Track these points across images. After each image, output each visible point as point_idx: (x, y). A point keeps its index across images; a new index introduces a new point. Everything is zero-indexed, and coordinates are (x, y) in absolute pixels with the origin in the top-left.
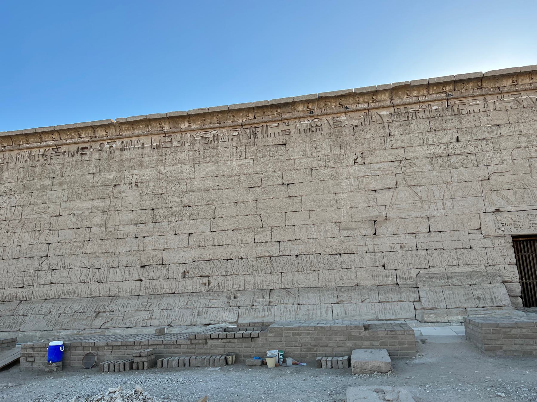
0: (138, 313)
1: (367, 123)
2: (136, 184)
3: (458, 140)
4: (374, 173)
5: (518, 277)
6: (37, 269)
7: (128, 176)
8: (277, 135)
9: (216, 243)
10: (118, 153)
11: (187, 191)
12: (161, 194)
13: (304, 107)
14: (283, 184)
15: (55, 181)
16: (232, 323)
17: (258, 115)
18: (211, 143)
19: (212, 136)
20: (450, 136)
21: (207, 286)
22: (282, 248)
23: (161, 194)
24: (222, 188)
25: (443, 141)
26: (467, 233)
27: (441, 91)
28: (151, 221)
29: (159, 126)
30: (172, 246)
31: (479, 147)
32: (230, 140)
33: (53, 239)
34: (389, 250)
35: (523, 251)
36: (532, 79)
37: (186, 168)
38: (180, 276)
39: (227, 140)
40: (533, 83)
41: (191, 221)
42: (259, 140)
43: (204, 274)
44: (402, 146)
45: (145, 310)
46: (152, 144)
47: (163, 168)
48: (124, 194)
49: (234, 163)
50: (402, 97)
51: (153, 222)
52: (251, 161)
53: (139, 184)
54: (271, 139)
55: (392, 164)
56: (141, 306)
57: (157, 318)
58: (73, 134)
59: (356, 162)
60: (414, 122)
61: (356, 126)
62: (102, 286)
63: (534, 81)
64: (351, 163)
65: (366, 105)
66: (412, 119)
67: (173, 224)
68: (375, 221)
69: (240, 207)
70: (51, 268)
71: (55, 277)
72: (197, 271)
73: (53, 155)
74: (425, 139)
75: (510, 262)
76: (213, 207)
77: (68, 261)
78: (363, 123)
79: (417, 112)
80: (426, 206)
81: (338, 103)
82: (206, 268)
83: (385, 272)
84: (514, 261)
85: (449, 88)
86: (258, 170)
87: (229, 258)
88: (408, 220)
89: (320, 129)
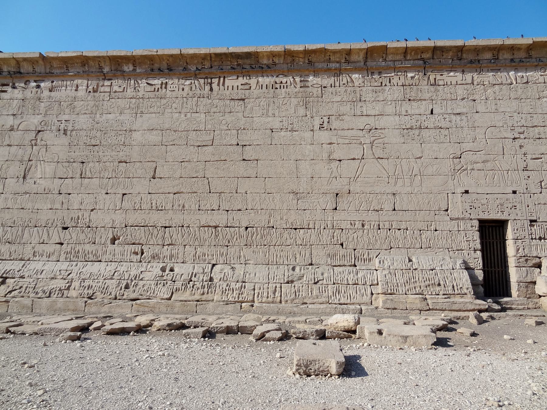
0: (53, 281)
1: (337, 84)
2: (65, 133)
3: (432, 113)
4: (340, 141)
5: (481, 264)
8: (235, 88)
9: (154, 208)
10: (46, 93)
11: (124, 145)
13: (269, 60)
14: (238, 145)
16: (164, 299)
17: (216, 63)
19: (160, 82)
20: (424, 107)
21: (139, 256)
22: (230, 218)
24: (166, 144)
25: (417, 112)
26: (432, 213)
27: (419, 57)
28: (78, 175)
29: (97, 66)
30: (101, 207)
31: (454, 122)
32: (181, 90)
34: (349, 226)
35: (487, 238)
36: (513, 54)
37: (126, 117)
38: (109, 242)
39: (177, 89)
41: (127, 179)
42: (215, 92)
43: (137, 242)
44: (373, 112)
45: (62, 278)
46: (88, 87)
47: (98, 116)
48: (48, 143)
49: (183, 116)
50: (377, 60)
52: (203, 116)
53: (69, 133)
54: (228, 93)
55: (360, 133)
56: (58, 273)
57: (76, 288)
59: (321, 127)
60: (387, 88)
61: (325, 87)
62: (13, 248)
63: (515, 56)
64: (317, 127)
65: (338, 65)
66: (386, 85)
67: (105, 181)
68: (337, 194)
69: (185, 168)
72: (129, 237)
74: (398, 108)
75: (474, 248)
76: (154, 166)
78: (333, 85)
79: (391, 78)
80: (392, 181)
81: (307, 59)
82: (140, 235)
83: (342, 252)
84: (479, 246)
85: (428, 56)
86: (210, 126)
87: (167, 225)
88: (372, 195)
89: (285, 87)
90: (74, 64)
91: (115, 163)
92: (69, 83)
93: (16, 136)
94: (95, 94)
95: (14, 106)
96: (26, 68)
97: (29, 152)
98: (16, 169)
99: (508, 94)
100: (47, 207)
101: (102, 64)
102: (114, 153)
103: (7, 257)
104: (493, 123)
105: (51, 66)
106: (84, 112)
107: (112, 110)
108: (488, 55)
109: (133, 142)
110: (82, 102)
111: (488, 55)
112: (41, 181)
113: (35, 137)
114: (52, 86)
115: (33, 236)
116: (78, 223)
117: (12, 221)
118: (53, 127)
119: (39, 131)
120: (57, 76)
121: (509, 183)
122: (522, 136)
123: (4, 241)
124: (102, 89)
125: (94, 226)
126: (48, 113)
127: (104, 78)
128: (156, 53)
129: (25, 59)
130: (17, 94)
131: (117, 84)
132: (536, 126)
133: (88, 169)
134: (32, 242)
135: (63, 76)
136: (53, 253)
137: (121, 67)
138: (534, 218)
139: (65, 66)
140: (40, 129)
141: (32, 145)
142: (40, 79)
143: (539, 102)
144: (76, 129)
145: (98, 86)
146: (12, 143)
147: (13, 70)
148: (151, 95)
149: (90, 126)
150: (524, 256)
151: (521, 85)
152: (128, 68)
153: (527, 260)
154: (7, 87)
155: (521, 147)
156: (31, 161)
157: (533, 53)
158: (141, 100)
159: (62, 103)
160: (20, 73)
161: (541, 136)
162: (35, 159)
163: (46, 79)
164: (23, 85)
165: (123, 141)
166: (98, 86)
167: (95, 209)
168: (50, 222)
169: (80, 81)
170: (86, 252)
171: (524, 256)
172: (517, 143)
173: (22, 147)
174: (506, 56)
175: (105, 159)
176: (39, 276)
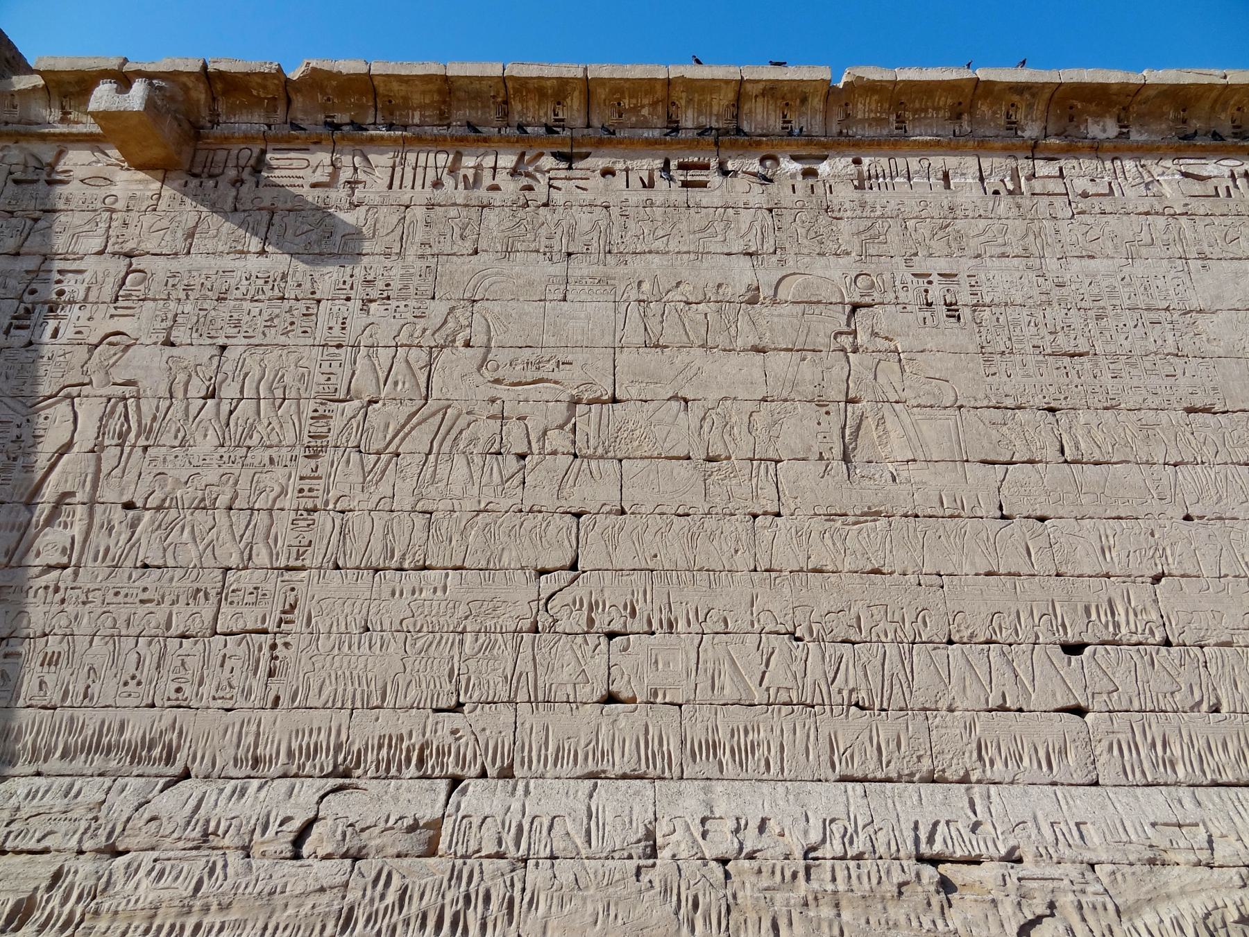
2: (952, 310)
6: (526, 624)
7: (909, 278)
10: (845, 194)
12: (1072, 356)
15: (580, 268)
18: (1229, 195)
23: (1072, 356)
28: (1052, 453)
29: (1002, 122)
33: (594, 491)
51: (1066, 461)
53: (966, 313)
58: (645, 112)
62: (885, 729)
70: (601, 623)
71: (633, 666)
73: (562, 174)
77: (688, 599)
90: (926, 110)
91: (1172, 414)
92: (914, 164)
93: (777, 322)
94: (1018, 199)
95: (744, 227)
96: (761, 117)
97: (839, 371)
98: (801, 429)
100: (973, 564)
101: (1020, 116)
102: (1154, 381)
103: (871, 768)
105: (848, 116)
106: (999, 250)
107: (1094, 247)
109: (1208, 347)
110: (982, 223)
112: (915, 473)
113: (848, 325)
114: (860, 173)
115: (965, 678)
116: (1117, 626)
117: (849, 617)
118: (902, 295)
119: (855, 307)
120: (875, 145)
123: (836, 698)
124: (1037, 185)
125: (1188, 638)
126: (871, 251)
127: (1030, 155)
128: (1223, 81)
129: (772, 90)
130: (744, 190)
131: (1082, 173)
133: (1080, 433)
134: (958, 703)
135: (895, 144)
136: (1063, 752)
137: (1078, 127)
139: (893, 118)
140: (857, 299)
141: (843, 350)
142: (815, 151)
144: (987, 300)
145: (1015, 177)
146: (766, 341)
147: (714, 125)
148: (1201, 207)
149: (1035, 292)
152: (1104, 131)
154: (706, 172)
156: (854, 401)
158: (1183, 221)
159: (911, 223)
160: (739, 131)
162: (871, 397)
163: (831, 153)
164: (755, 166)
165: (1170, 341)
166: (1015, 177)
167: (1163, 575)
168: (1008, 621)
169: (951, 162)
170: (1200, 744)
173: (809, 355)
175: (1131, 400)
176: (1088, 856)
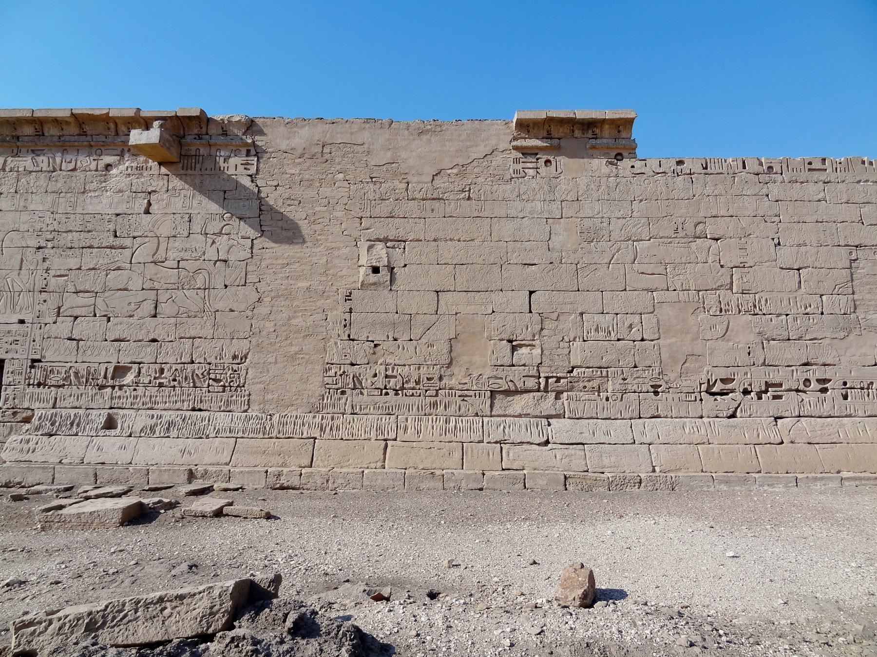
40: (63, 136)
63: (65, 132)
99: (45, 185)
104: (17, 226)
108: (28, 130)
111: (28, 130)
121: (18, 308)
122: (50, 245)
132: (71, 231)
138: (38, 357)
143: (81, 198)
150: (13, 408)
151: (65, 173)
153: (15, 414)
155: (44, 260)
157: (87, 128)
161: (73, 245)
171: (13, 408)
172: (40, 255)
174: (52, 131)
